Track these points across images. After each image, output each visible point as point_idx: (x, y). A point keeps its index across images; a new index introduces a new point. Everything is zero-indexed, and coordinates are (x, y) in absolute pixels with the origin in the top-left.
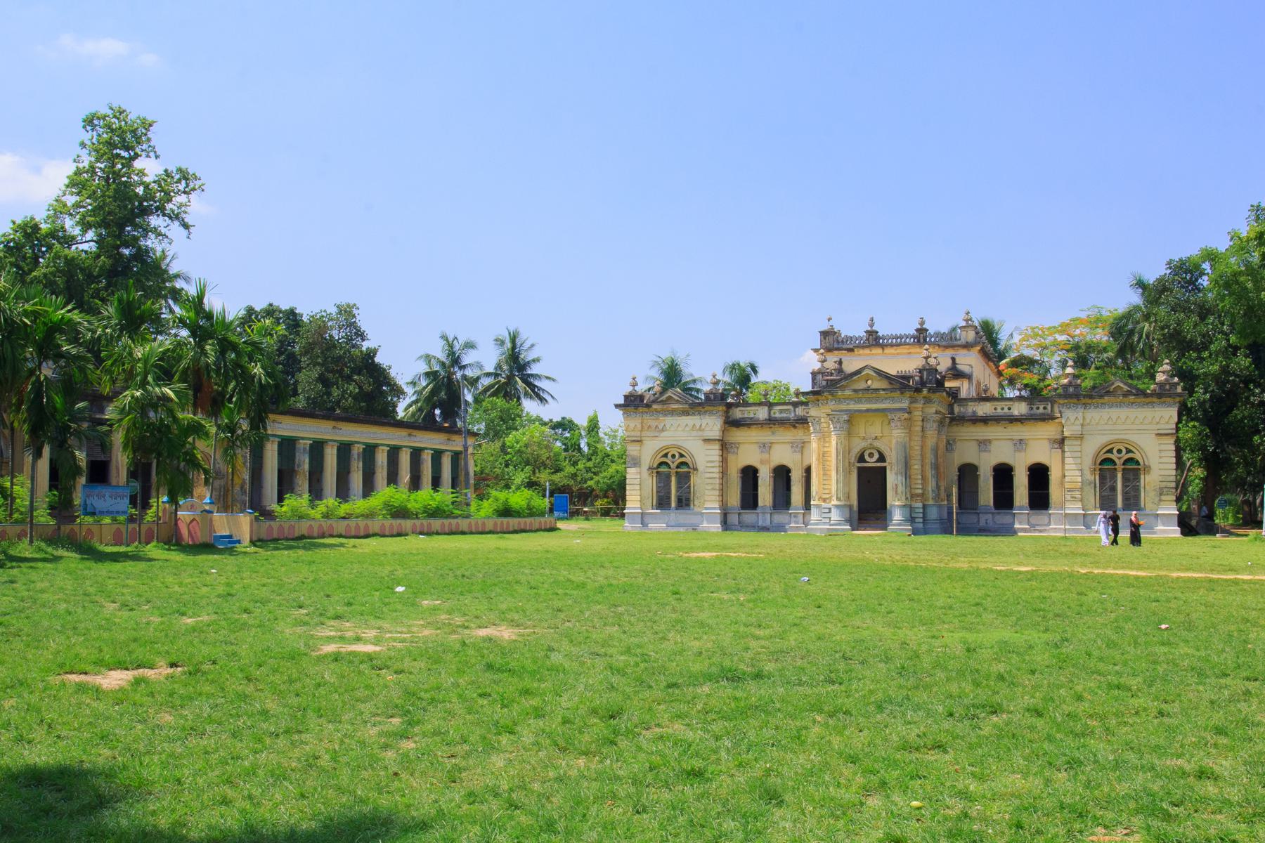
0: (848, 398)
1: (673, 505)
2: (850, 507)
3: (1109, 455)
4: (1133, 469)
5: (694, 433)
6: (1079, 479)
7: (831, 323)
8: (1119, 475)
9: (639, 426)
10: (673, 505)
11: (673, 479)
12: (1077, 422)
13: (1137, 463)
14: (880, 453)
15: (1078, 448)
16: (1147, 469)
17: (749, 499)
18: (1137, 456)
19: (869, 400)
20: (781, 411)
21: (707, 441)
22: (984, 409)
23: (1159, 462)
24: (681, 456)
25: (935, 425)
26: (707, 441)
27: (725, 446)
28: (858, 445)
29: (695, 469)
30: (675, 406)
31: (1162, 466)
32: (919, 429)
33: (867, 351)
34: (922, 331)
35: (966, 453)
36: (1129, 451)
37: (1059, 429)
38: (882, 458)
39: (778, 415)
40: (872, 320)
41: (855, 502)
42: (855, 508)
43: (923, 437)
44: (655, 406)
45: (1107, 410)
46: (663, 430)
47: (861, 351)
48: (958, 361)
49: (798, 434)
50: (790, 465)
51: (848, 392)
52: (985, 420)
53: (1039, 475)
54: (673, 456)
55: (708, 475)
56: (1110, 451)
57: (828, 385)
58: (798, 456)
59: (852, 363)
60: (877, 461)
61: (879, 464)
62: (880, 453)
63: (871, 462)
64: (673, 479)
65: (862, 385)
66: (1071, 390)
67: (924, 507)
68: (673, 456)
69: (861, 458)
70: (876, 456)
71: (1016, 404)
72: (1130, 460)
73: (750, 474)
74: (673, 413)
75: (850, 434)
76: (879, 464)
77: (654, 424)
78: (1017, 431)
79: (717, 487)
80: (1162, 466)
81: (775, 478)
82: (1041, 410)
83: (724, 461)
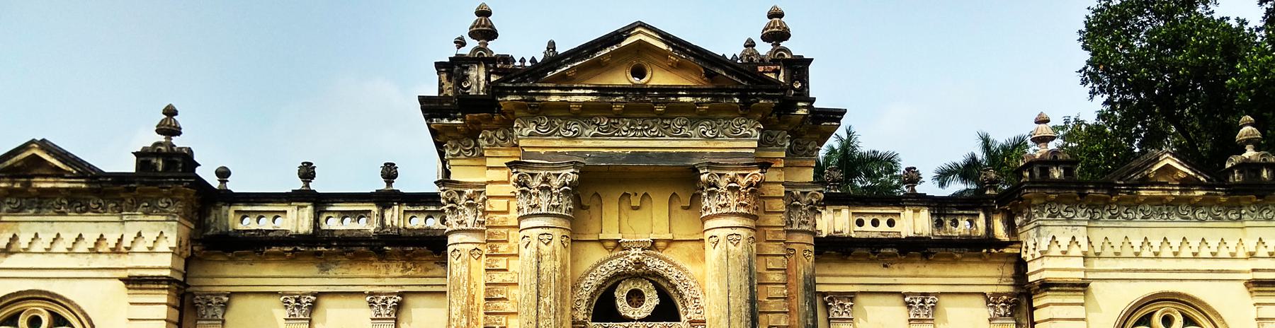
0: (584, 114)
12: (1075, 250)
15: (1078, 312)
20: (344, 215)
21: (135, 282)
26: (135, 282)
28: (596, 264)
37: (1009, 271)
43: (789, 253)
49: (388, 278)
62: (662, 294)
66: (1056, 174)
70: (652, 301)
71: (908, 213)
74: (43, 202)
75: (575, 239)
82: (963, 227)
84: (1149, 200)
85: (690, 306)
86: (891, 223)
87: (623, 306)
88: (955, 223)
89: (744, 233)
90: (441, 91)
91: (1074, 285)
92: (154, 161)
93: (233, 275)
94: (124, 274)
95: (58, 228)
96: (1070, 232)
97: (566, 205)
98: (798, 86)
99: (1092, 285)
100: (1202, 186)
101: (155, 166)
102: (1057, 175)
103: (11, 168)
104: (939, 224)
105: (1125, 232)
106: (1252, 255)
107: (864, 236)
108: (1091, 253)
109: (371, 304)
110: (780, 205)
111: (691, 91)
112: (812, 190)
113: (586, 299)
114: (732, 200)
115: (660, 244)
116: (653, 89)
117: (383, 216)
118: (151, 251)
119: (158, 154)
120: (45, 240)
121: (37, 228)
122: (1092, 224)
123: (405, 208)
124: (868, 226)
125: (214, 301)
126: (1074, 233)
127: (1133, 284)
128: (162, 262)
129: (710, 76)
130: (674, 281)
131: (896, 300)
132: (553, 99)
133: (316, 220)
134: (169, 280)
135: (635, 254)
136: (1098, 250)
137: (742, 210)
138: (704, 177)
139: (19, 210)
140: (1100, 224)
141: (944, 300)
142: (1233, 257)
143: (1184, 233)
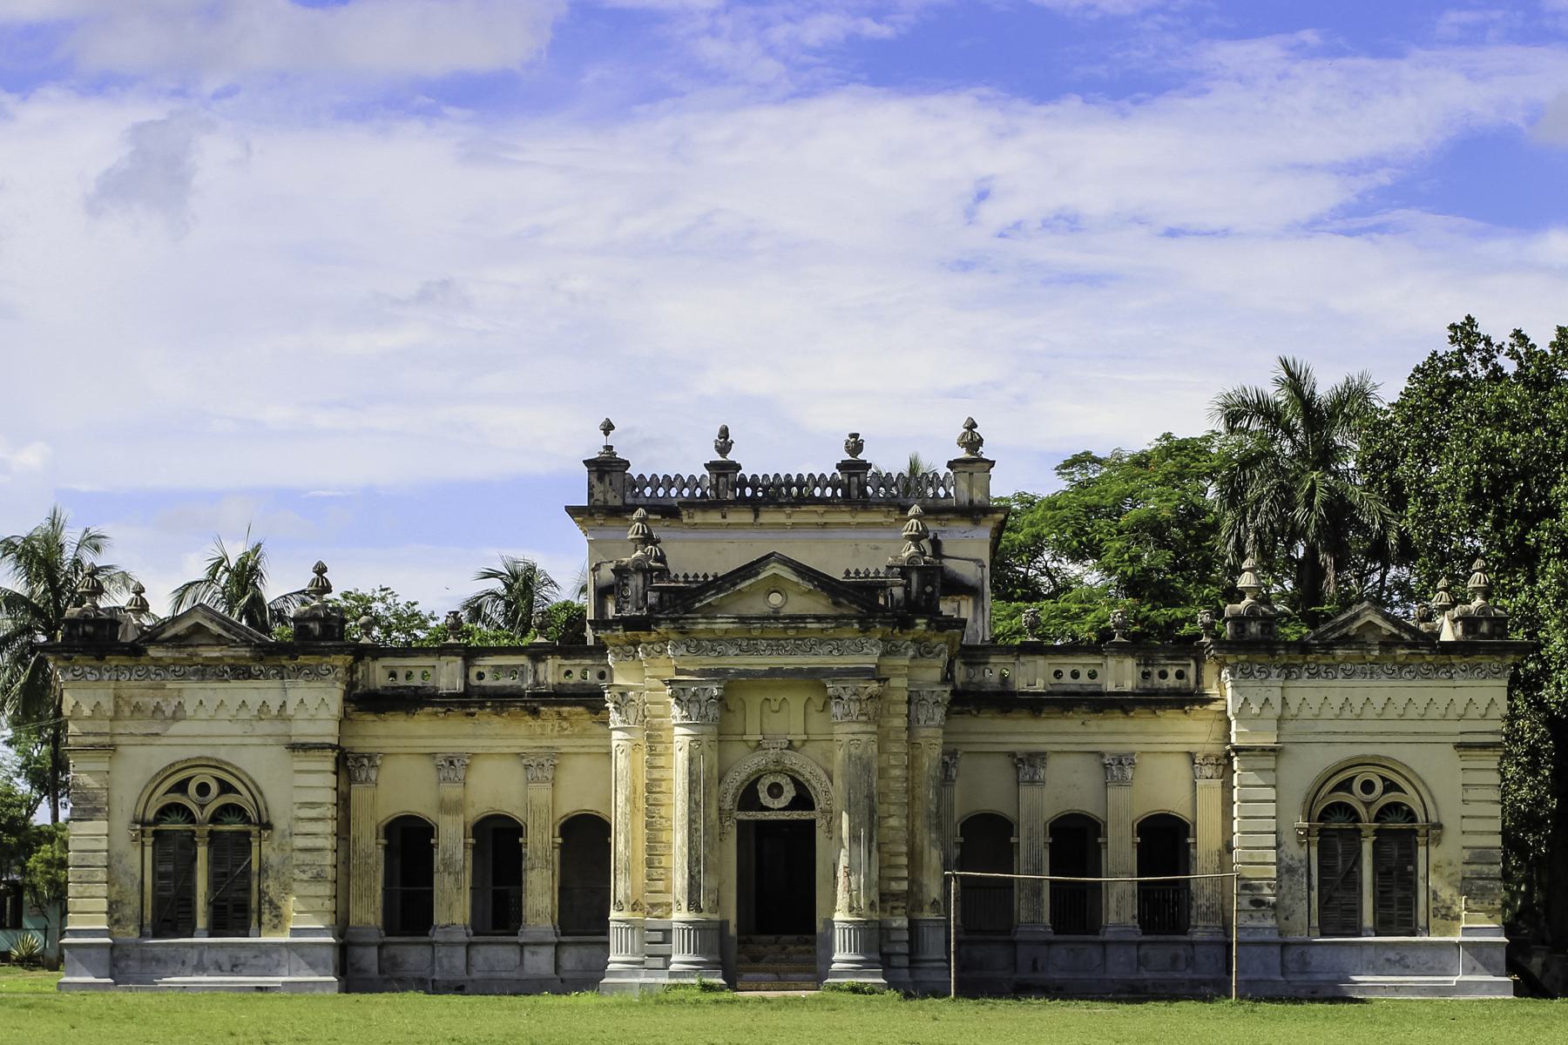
0: (725, 639)
1: (201, 922)
2: (723, 924)
3: (1342, 797)
4: (1402, 833)
5: (265, 727)
6: (1271, 856)
7: (612, 439)
8: (1367, 847)
9: (108, 706)
10: (201, 922)
11: (202, 852)
12: (1268, 713)
13: (1410, 815)
14: (797, 784)
16: (1436, 830)
17: (410, 907)
18: (1411, 799)
19: (777, 646)
20: (497, 669)
22: (1033, 676)
23: (1466, 806)
24: (226, 788)
25: (939, 713)
27: (349, 764)
29: (268, 826)
30: (215, 653)
31: (1469, 825)
32: (900, 722)
33: (714, 517)
34: (854, 467)
35: (986, 789)
36: (1390, 786)
37: (1218, 728)
38: (804, 800)
39: (488, 681)
40: (724, 433)
41: (732, 917)
42: (733, 930)
44: (153, 652)
45: (1340, 682)
46: (175, 718)
47: (699, 518)
48: (946, 551)
50: (518, 815)
51: (721, 625)
52: (1036, 705)
53: (1165, 839)
54: (203, 789)
55: (300, 842)
56: (1345, 786)
57: (657, 605)
58: (541, 793)
59: (694, 553)
60: (792, 806)
61: (795, 815)
62: (797, 784)
63: (776, 808)
64: (202, 852)
65: (757, 606)
67: (914, 926)
68: (203, 789)
69: (748, 798)
70: (789, 793)
71: (1111, 662)
72: (1394, 807)
73: (410, 841)
74: (206, 671)
75: (723, 738)
76: (795, 815)
77: (150, 700)
78: (1113, 733)
79: (330, 873)
80: (1469, 825)
81: (477, 849)
82: (1171, 681)
83: (343, 802)
84: (1346, 659)
85: (822, 797)
86: (1092, 675)
87: (765, 799)
88: (1163, 675)
89: (864, 738)
90: (590, 495)
91: (1263, 749)
92: (311, 625)
93: (383, 733)
94: (286, 740)
95: (221, 696)
96: (1264, 693)
97: (713, 712)
98: (929, 589)
99: (1288, 747)
100: (1408, 645)
101: (311, 631)
102: (1253, 630)
103: (176, 637)
104: (1146, 675)
105: (1324, 692)
106: (1460, 718)
107: (1062, 689)
108: (1287, 715)
109: (527, 767)
110: (904, 709)
111: (819, 619)
112: (938, 689)
113: (732, 791)
114: (855, 708)
115: (796, 744)
116: (785, 618)
117: (536, 672)
118: (312, 719)
119: (315, 618)
120: (210, 706)
121: (201, 696)
122: (1289, 683)
123: (559, 661)
124: (1067, 679)
125: (366, 761)
126: (1268, 694)
127: (1331, 748)
128: (324, 727)
129: (836, 604)
130: (808, 776)
131: (1093, 757)
132: (701, 627)
133: (467, 676)
134: (332, 747)
135: (772, 754)
136: (1294, 710)
137: (863, 718)
138: (830, 691)
139: (183, 677)
140: (1298, 683)
141: (1146, 758)
142: (1444, 718)
143: (1387, 692)
